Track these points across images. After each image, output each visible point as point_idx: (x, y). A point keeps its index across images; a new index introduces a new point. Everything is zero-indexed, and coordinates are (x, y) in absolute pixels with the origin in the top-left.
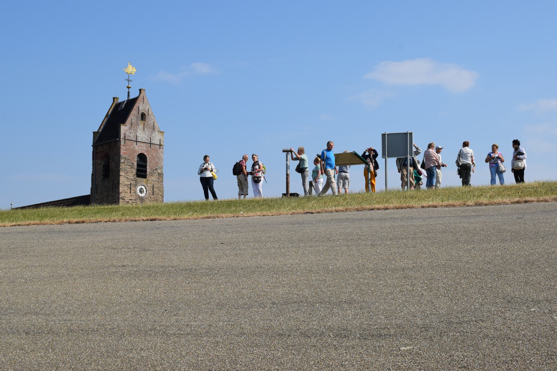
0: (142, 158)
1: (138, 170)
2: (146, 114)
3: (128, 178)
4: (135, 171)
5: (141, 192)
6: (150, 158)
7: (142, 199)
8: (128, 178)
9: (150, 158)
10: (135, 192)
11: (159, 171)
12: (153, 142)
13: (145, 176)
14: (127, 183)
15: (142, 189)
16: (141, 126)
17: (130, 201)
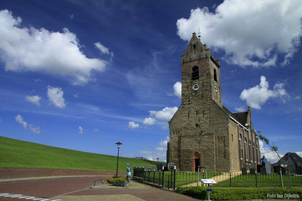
0: (195, 68)
1: (193, 76)
2: (196, 44)
3: (186, 83)
4: (191, 78)
5: (195, 88)
6: (200, 67)
7: (196, 91)
8: (186, 83)
9: (200, 67)
10: (191, 89)
11: (208, 72)
12: (201, 57)
13: (198, 78)
14: (186, 85)
15: (196, 86)
16: (193, 53)
17: (188, 95)
